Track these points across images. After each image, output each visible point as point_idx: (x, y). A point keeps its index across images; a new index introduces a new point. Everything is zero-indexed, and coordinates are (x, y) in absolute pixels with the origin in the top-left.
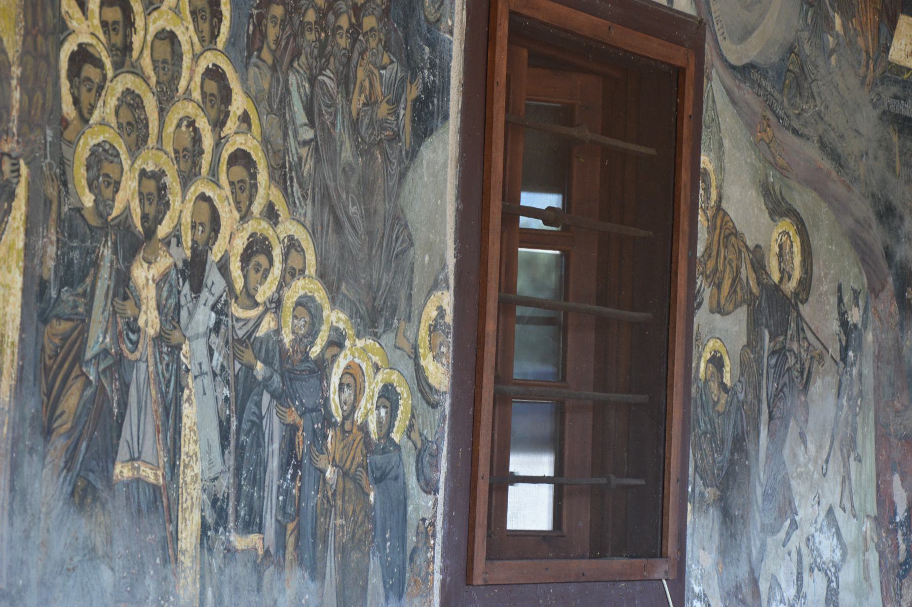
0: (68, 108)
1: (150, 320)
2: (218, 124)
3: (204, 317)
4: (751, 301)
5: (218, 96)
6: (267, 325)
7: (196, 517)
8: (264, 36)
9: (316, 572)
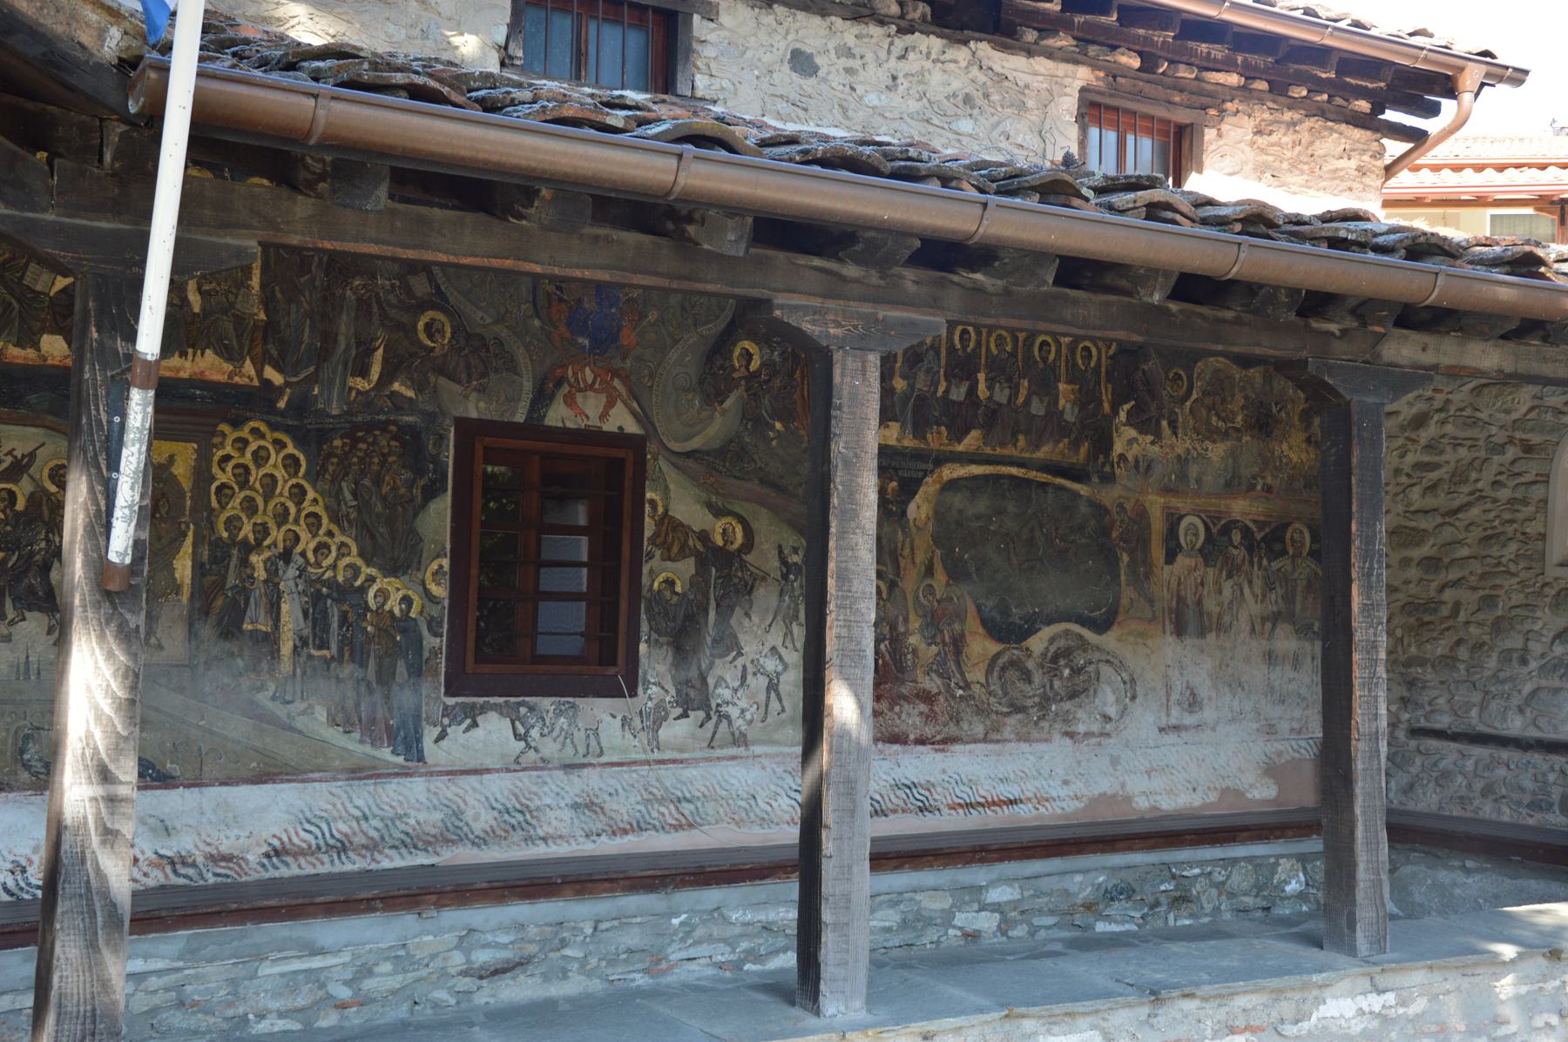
0: (214, 504)
1: (261, 574)
2: (299, 504)
3: (292, 572)
4: (697, 555)
5: (299, 494)
6: (329, 574)
7: (291, 643)
8: (326, 470)
9: (363, 664)
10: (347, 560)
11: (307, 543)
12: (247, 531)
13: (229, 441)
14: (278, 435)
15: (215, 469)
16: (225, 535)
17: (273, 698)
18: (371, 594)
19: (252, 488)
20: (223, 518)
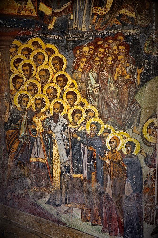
0: (12, 88)
1: (40, 129)
3: (59, 128)
6: (81, 129)
7: (59, 170)
10: (92, 120)
11: (68, 110)
12: (31, 103)
13: (20, 50)
14: (49, 46)
15: (12, 67)
16: (18, 106)
17: (48, 203)
18: (108, 140)
19: (34, 78)
20: (17, 96)
